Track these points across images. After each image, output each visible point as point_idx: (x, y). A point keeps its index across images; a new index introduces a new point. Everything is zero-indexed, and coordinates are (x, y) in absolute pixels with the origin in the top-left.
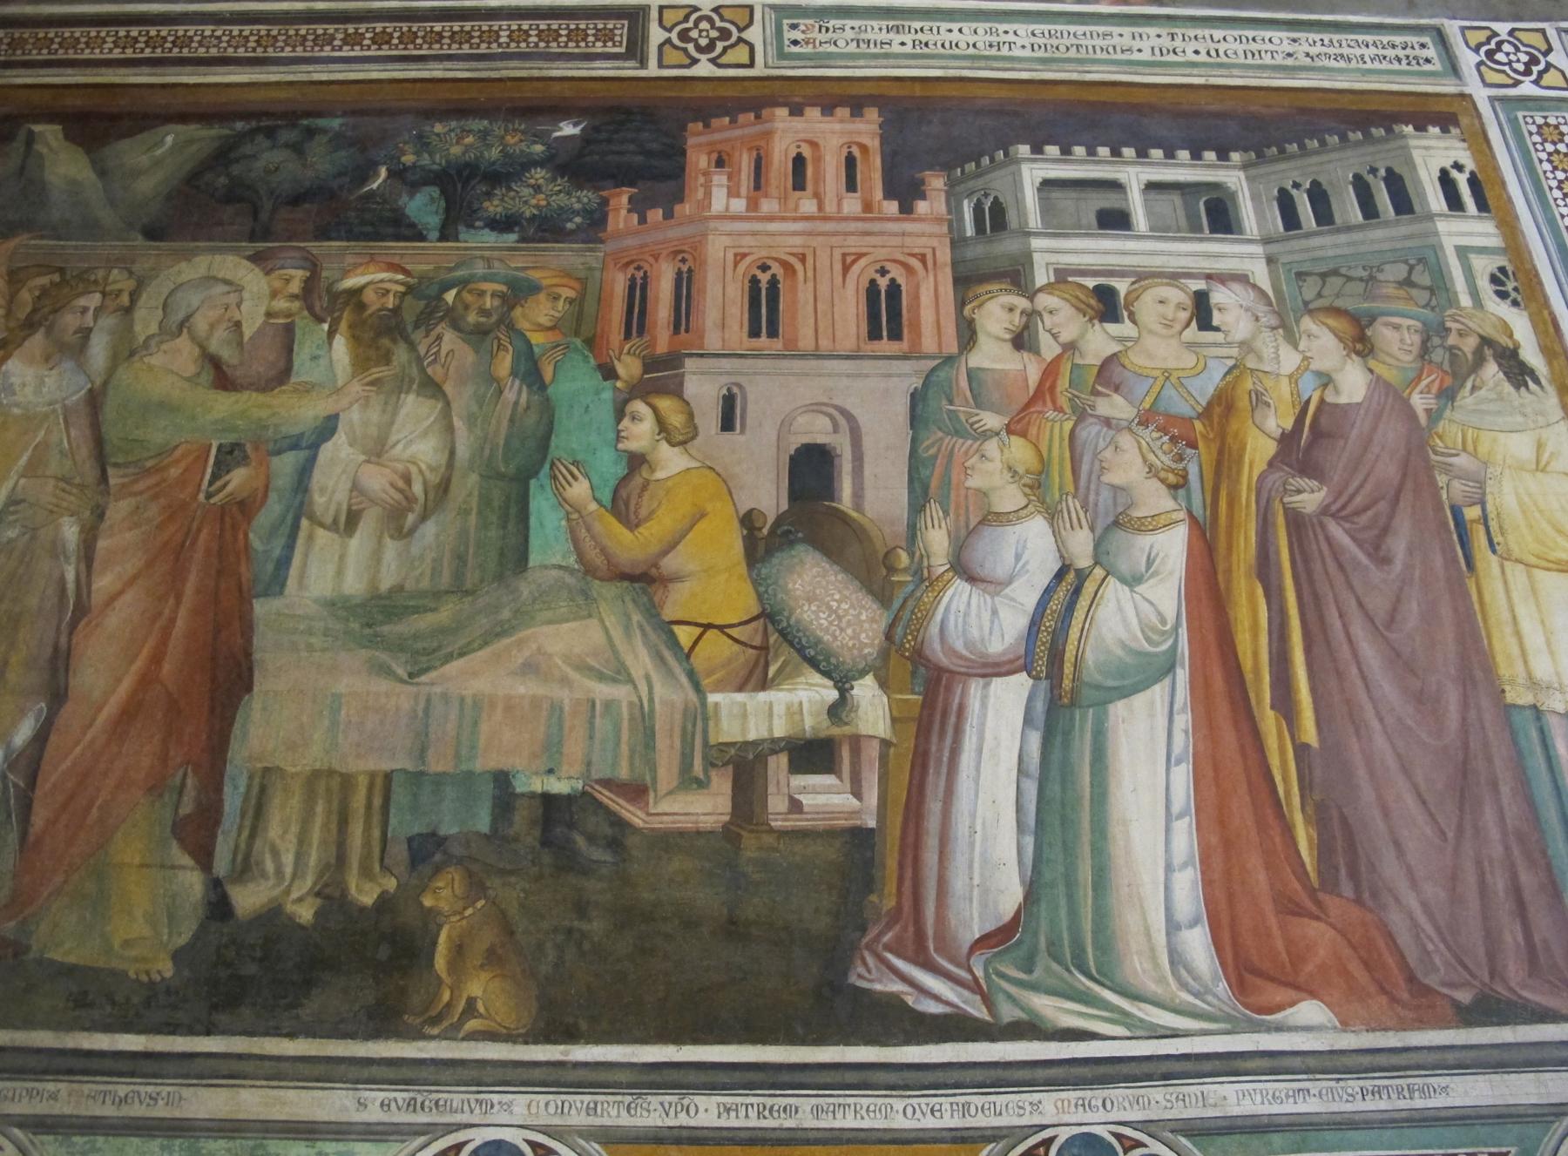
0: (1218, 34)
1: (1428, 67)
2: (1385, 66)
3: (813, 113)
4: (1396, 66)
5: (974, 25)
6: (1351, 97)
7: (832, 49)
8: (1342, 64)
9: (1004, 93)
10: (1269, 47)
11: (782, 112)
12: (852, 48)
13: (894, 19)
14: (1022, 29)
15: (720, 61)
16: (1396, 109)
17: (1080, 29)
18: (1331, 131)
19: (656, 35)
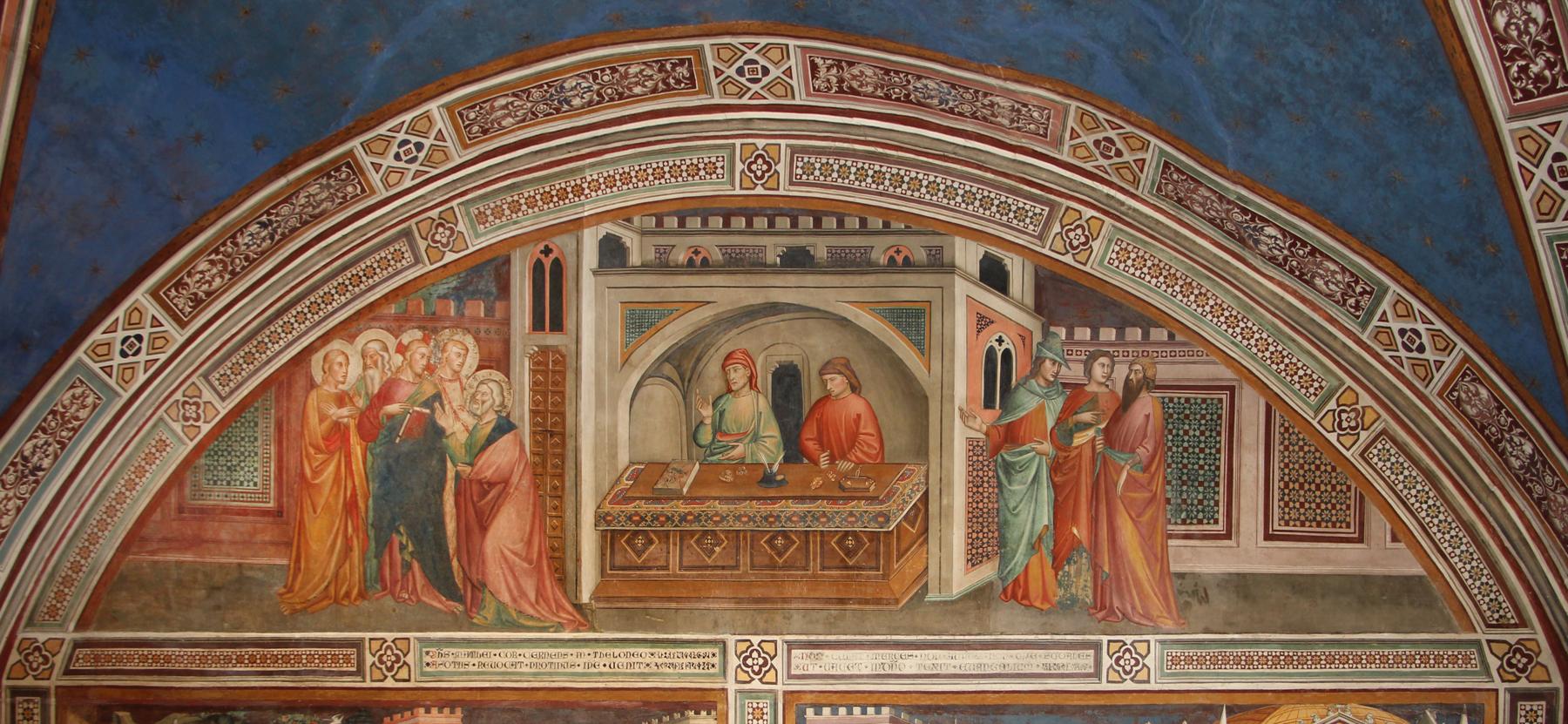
0: (617, 651)
1: (712, 671)
2: (692, 670)
3: (434, 711)
4: (697, 671)
5: (506, 650)
6: (670, 693)
7: (442, 668)
8: (671, 671)
9: (513, 697)
10: (640, 660)
11: (422, 710)
12: (451, 669)
13: (471, 647)
14: (527, 652)
15: (396, 677)
16: (689, 700)
17: (552, 651)
18: (655, 716)
19: (369, 659)
